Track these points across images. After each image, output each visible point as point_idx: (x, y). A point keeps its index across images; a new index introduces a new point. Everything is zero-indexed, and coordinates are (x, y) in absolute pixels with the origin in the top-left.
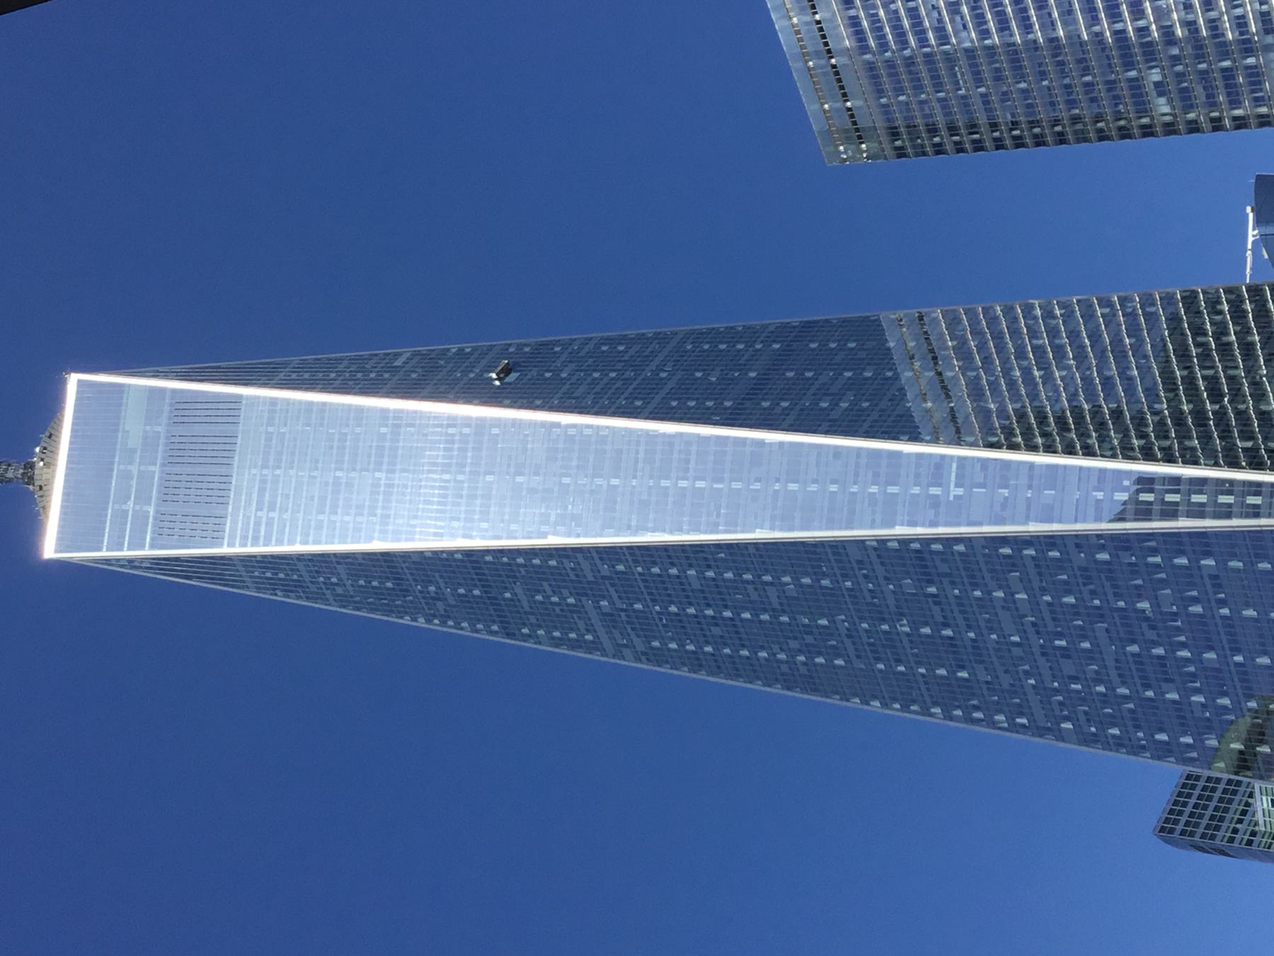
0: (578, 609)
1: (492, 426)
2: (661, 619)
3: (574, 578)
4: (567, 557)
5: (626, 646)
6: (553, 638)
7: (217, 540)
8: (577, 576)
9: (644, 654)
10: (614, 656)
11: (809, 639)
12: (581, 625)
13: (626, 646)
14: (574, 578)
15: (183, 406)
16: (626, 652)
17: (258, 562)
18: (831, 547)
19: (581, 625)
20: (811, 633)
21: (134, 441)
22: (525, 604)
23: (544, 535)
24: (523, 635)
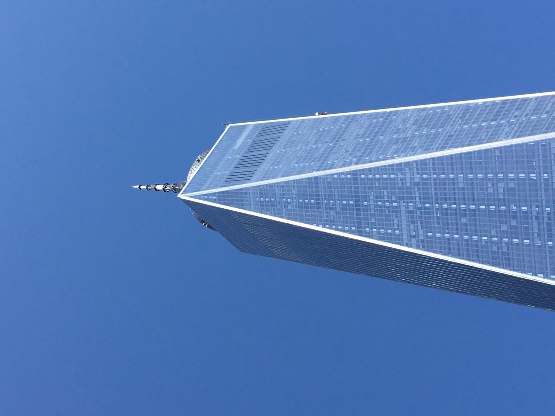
0: (396, 211)
1: (394, 115)
2: (437, 214)
3: (400, 185)
4: (401, 170)
5: (414, 237)
6: (380, 233)
7: (248, 180)
8: (402, 183)
9: (423, 241)
10: (407, 245)
11: (514, 223)
12: (396, 222)
13: (414, 237)
14: (400, 185)
15: (265, 130)
16: (414, 241)
17: (261, 190)
18: (543, 145)
19: (396, 222)
20: (515, 217)
21: (236, 147)
22: (372, 207)
23: (392, 158)
24: (366, 232)
